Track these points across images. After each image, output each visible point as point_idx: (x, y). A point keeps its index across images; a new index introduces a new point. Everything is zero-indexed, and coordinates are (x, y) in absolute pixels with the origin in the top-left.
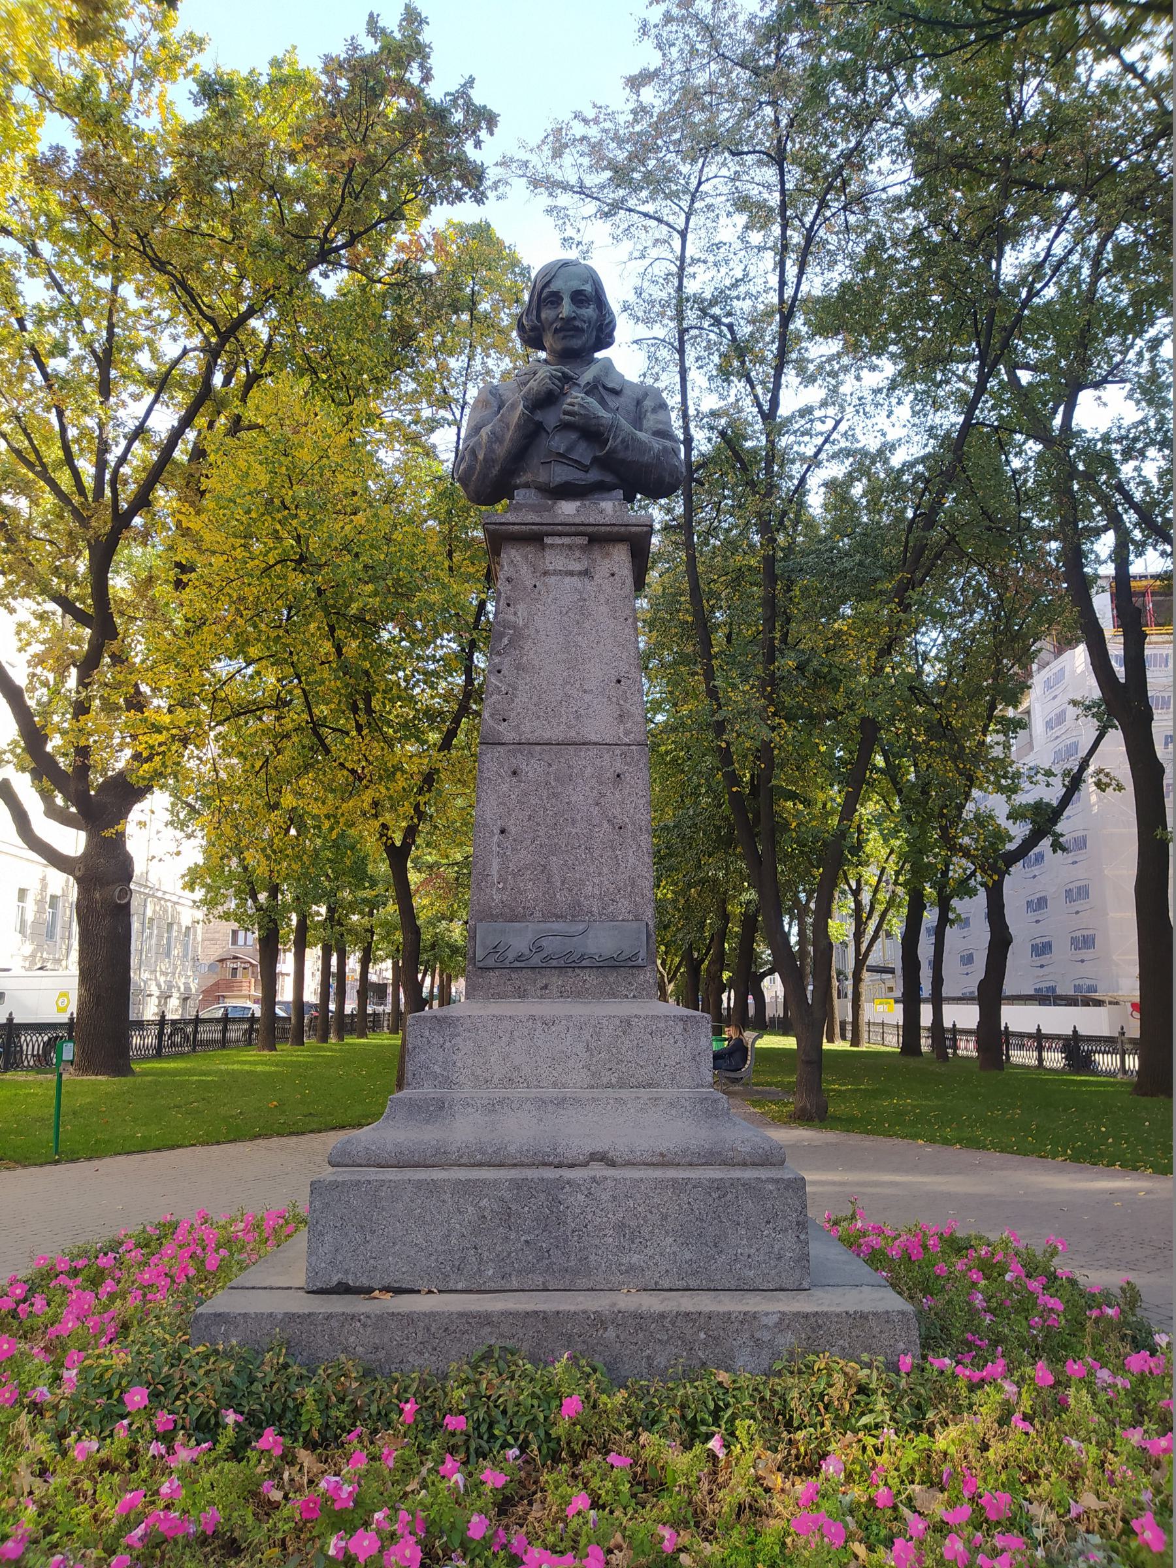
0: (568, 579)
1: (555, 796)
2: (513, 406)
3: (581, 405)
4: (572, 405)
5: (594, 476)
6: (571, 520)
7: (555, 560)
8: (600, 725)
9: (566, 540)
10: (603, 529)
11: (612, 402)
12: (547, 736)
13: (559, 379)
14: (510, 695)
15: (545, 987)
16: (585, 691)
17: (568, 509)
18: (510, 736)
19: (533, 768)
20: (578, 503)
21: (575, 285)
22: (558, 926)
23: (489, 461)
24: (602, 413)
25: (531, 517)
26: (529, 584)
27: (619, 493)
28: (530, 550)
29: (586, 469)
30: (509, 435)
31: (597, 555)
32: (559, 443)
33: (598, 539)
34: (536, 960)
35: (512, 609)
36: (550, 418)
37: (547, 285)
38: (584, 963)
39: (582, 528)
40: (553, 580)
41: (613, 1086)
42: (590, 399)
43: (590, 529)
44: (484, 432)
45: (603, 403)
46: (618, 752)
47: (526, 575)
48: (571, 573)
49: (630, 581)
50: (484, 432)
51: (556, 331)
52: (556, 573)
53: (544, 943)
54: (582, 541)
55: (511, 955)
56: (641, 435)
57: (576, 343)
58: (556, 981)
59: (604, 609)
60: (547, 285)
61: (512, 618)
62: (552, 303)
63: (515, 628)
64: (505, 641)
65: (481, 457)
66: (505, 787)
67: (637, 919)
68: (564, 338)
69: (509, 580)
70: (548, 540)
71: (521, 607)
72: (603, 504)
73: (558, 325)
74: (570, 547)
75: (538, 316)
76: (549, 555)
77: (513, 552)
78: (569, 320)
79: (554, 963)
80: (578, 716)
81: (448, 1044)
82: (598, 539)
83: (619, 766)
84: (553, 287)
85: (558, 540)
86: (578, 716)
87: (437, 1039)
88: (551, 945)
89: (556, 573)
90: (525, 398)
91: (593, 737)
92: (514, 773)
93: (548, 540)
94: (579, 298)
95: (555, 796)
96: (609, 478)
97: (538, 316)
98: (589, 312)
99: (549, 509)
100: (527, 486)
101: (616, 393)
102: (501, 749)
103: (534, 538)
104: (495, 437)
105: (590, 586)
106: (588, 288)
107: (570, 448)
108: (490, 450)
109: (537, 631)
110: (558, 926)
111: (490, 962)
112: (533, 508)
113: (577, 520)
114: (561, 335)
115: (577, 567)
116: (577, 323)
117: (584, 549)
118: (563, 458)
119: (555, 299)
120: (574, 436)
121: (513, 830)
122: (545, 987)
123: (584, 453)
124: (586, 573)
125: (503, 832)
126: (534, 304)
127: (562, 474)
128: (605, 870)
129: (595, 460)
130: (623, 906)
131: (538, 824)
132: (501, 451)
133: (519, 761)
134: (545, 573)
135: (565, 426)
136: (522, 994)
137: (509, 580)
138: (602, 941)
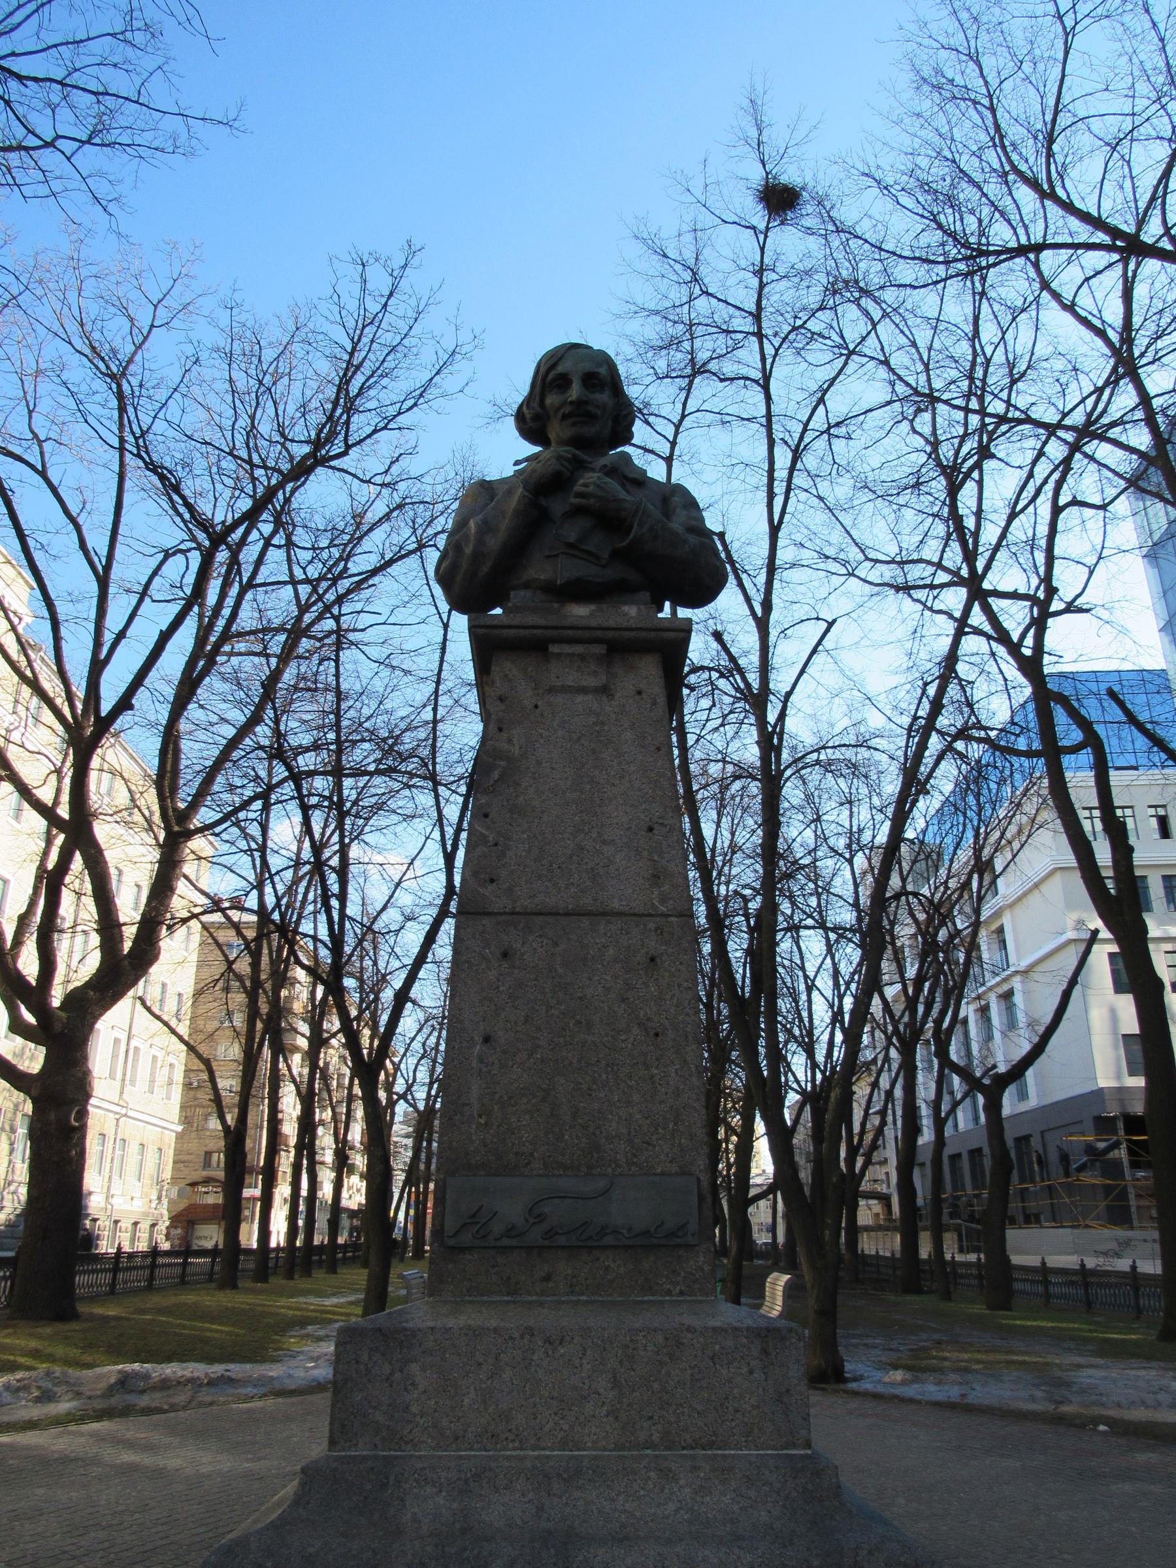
0: (580, 698)
3: (598, 486)
4: (586, 485)
6: (583, 623)
9: (579, 649)
10: (627, 634)
13: (568, 460)
15: (547, 1278)
16: (604, 842)
17: (580, 612)
18: (501, 904)
20: (593, 607)
21: (587, 366)
23: (478, 557)
25: (532, 619)
27: (646, 596)
30: (504, 526)
32: (572, 532)
33: (620, 648)
35: (505, 735)
36: (557, 506)
37: (553, 367)
38: (608, 1240)
39: (599, 633)
40: (559, 699)
41: (654, 1447)
43: (610, 634)
46: (652, 926)
48: (583, 690)
49: (662, 700)
51: (565, 417)
52: (564, 690)
54: (599, 649)
55: (497, 1228)
57: (590, 431)
59: (628, 735)
60: (553, 367)
61: (505, 746)
62: (559, 387)
64: (496, 775)
65: (468, 550)
66: (492, 975)
68: (574, 424)
69: (501, 699)
70: (554, 649)
72: (626, 608)
73: (567, 409)
74: (582, 657)
75: (542, 403)
77: (508, 665)
78: (579, 403)
79: (562, 1240)
81: (397, 1375)
84: (560, 369)
85: (567, 649)
89: (564, 690)
91: (616, 904)
92: (505, 955)
93: (554, 649)
97: (542, 403)
98: (604, 397)
100: (527, 585)
102: (486, 921)
104: (486, 528)
106: (603, 371)
108: (480, 541)
109: (539, 763)
113: (593, 623)
114: (570, 421)
115: (591, 682)
116: (590, 408)
119: (563, 382)
122: (547, 1278)
124: (605, 690)
125: (487, 1040)
126: (538, 390)
128: (636, 1097)
129: (616, 554)
131: (539, 1029)
132: (494, 543)
134: (551, 690)
135: (579, 511)
137: (501, 699)
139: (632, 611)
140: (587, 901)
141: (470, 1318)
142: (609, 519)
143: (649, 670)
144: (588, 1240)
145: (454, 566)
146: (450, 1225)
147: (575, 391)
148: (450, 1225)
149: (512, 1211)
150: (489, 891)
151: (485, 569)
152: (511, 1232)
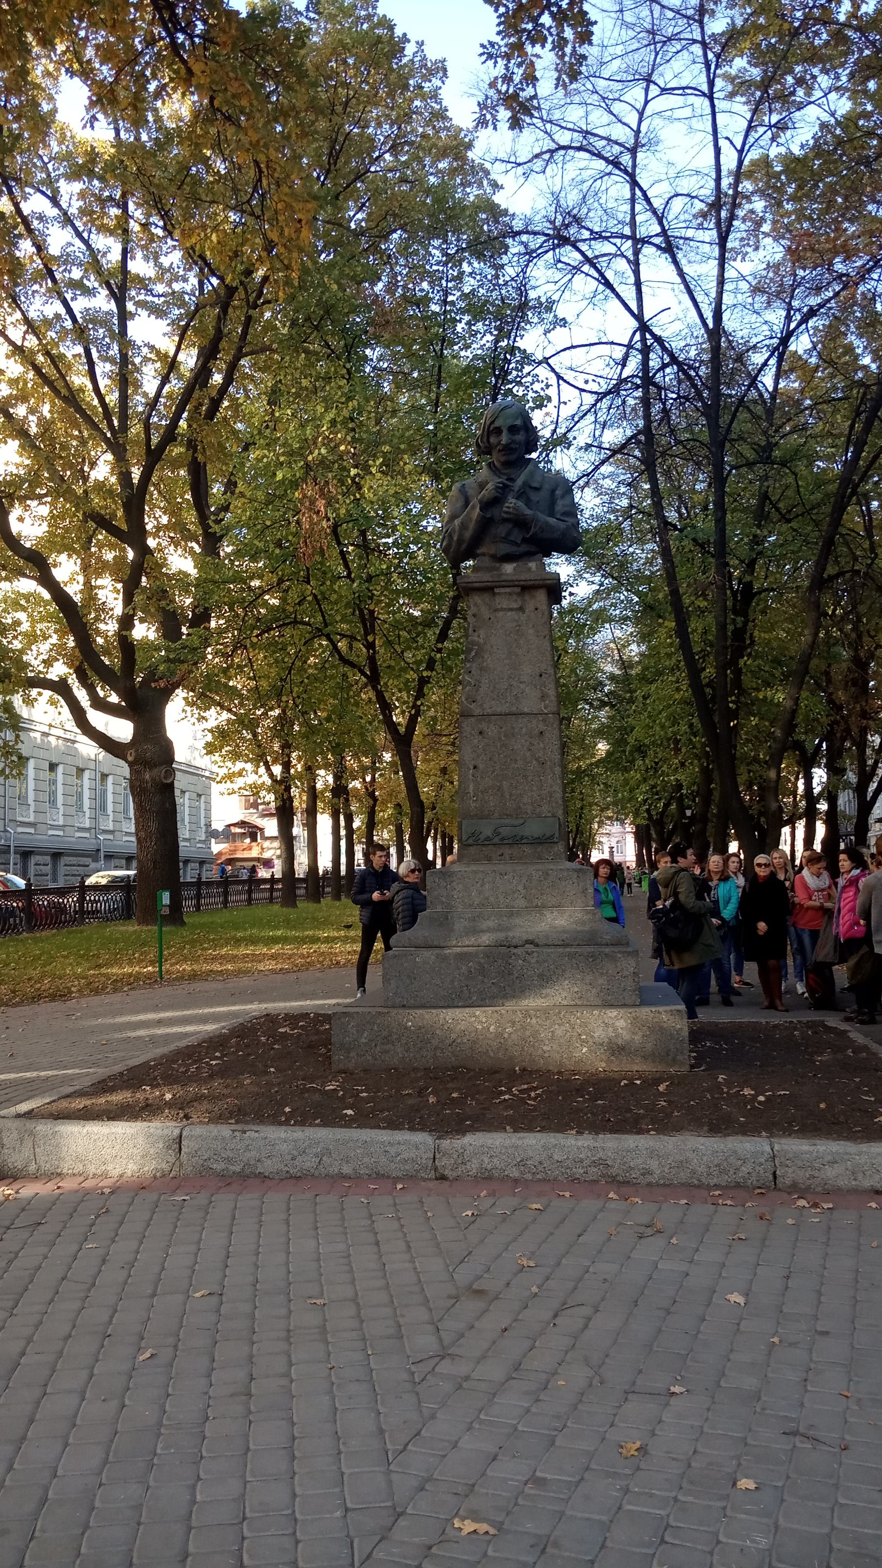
1: (504, 745)
2: (473, 507)
5: (524, 548)
7: (502, 602)
8: (530, 703)
9: (508, 590)
11: (534, 497)
12: (499, 710)
14: (477, 686)
17: (509, 568)
18: (477, 711)
19: (492, 730)
21: (510, 422)
22: (508, 821)
23: (460, 541)
24: (528, 512)
26: (487, 617)
28: (486, 596)
29: (518, 545)
30: (472, 526)
31: (527, 597)
33: (526, 588)
34: (496, 840)
36: (495, 512)
40: (501, 614)
42: (520, 503)
44: (457, 522)
45: (528, 503)
47: (485, 613)
48: (511, 610)
50: (457, 522)
52: (502, 609)
53: (501, 830)
54: (518, 590)
55: (482, 837)
56: (552, 521)
57: (513, 457)
58: (507, 851)
59: (531, 631)
63: (478, 644)
67: (554, 816)
71: (482, 632)
76: (498, 599)
80: (516, 697)
82: (526, 588)
83: (542, 727)
84: (497, 424)
85: (503, 590)
86: (516, 697)
87: (443, 884)
88: (505, 831)
89: (502, 609)
90: (480, 502)
91: (526, 710)
94: (513, 429)
95: (504, 745)
96: (533, 549)
98: (520, 437)
99: (498, 569)
100: (484, 554)
101: (537, 489)
103: (488, 589)
104: (463, 526)
105: (523, 617)
107: (509, 533)
108: (461, 535)
110: (508, 821)
111: (471, 841)
112: (489, 569)
115: (515, 606)
117: (518, 594)
118: (505, 539)
119: (498, 431)
120: (510, 526)
121: (481, 766)
123: (517, 536)
124: (521, 609)
127: (504, 549)
129: (524, 540)
130: (545, 809)
132: (468, 534)
133: (483, 726)
134: (496, 610)
135: (505, 520)
136: (489, 859)
138: (533, 829)
139: (533, 565)
140: (514, 709)
141: (473, 868)
142: (520, 523)
143: (541, 596)
144: (516, 841)
145: (449, 546)
146: (464, 838)
147: (504, 438)
148: (464, 838)
149: (488, 832)
150: (472, 706)
151: (464, 546)
152: (488, 839)
